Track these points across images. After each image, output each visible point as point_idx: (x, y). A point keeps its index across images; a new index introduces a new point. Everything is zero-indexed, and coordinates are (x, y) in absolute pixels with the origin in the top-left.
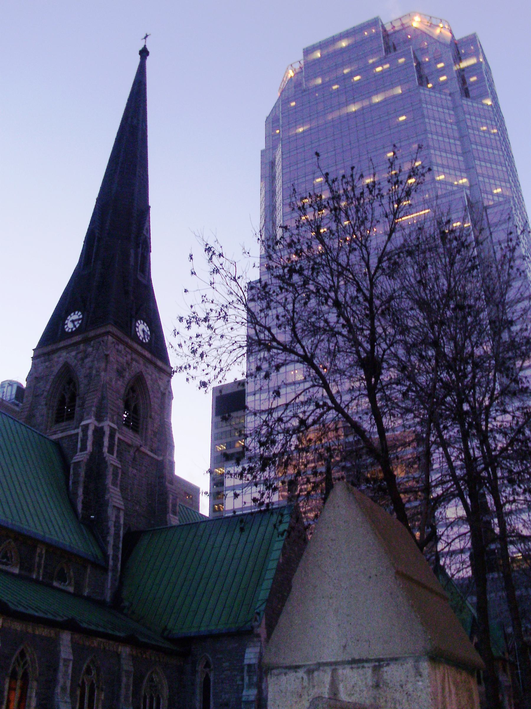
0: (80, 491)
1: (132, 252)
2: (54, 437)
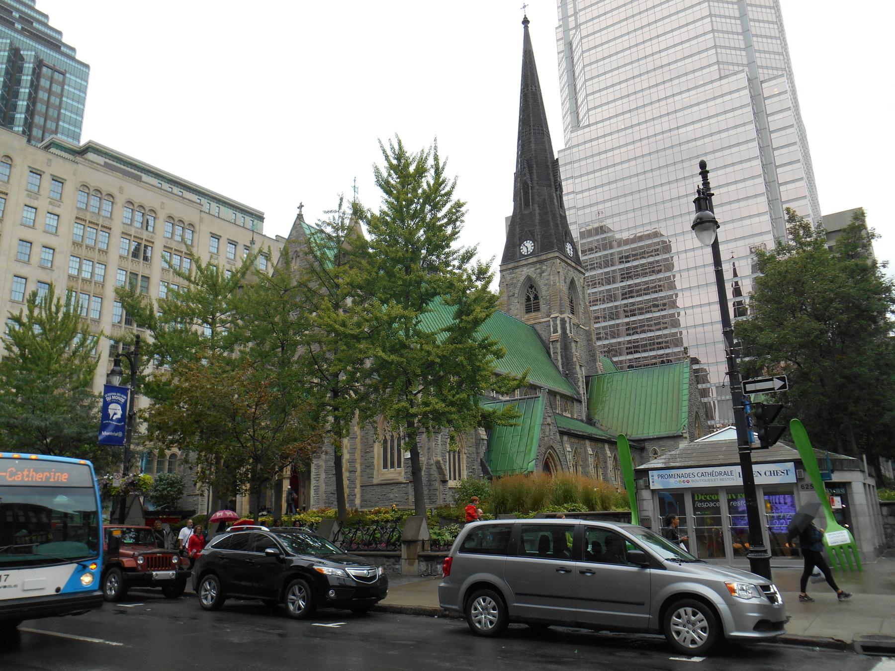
0: (559, 358)
1: (554, 195)
2: (529, 323)
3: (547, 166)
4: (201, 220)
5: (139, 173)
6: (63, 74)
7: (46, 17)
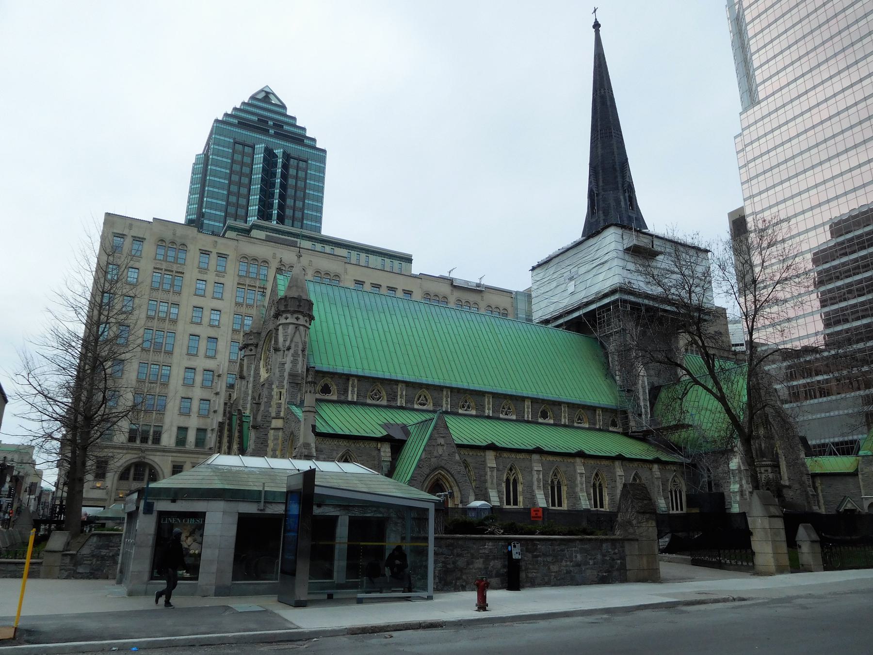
1: (622, 197)
3: (615, 169)
4: (346, 271)
5: (295, 239)
6: (306, 161)
7: (294, 119)
